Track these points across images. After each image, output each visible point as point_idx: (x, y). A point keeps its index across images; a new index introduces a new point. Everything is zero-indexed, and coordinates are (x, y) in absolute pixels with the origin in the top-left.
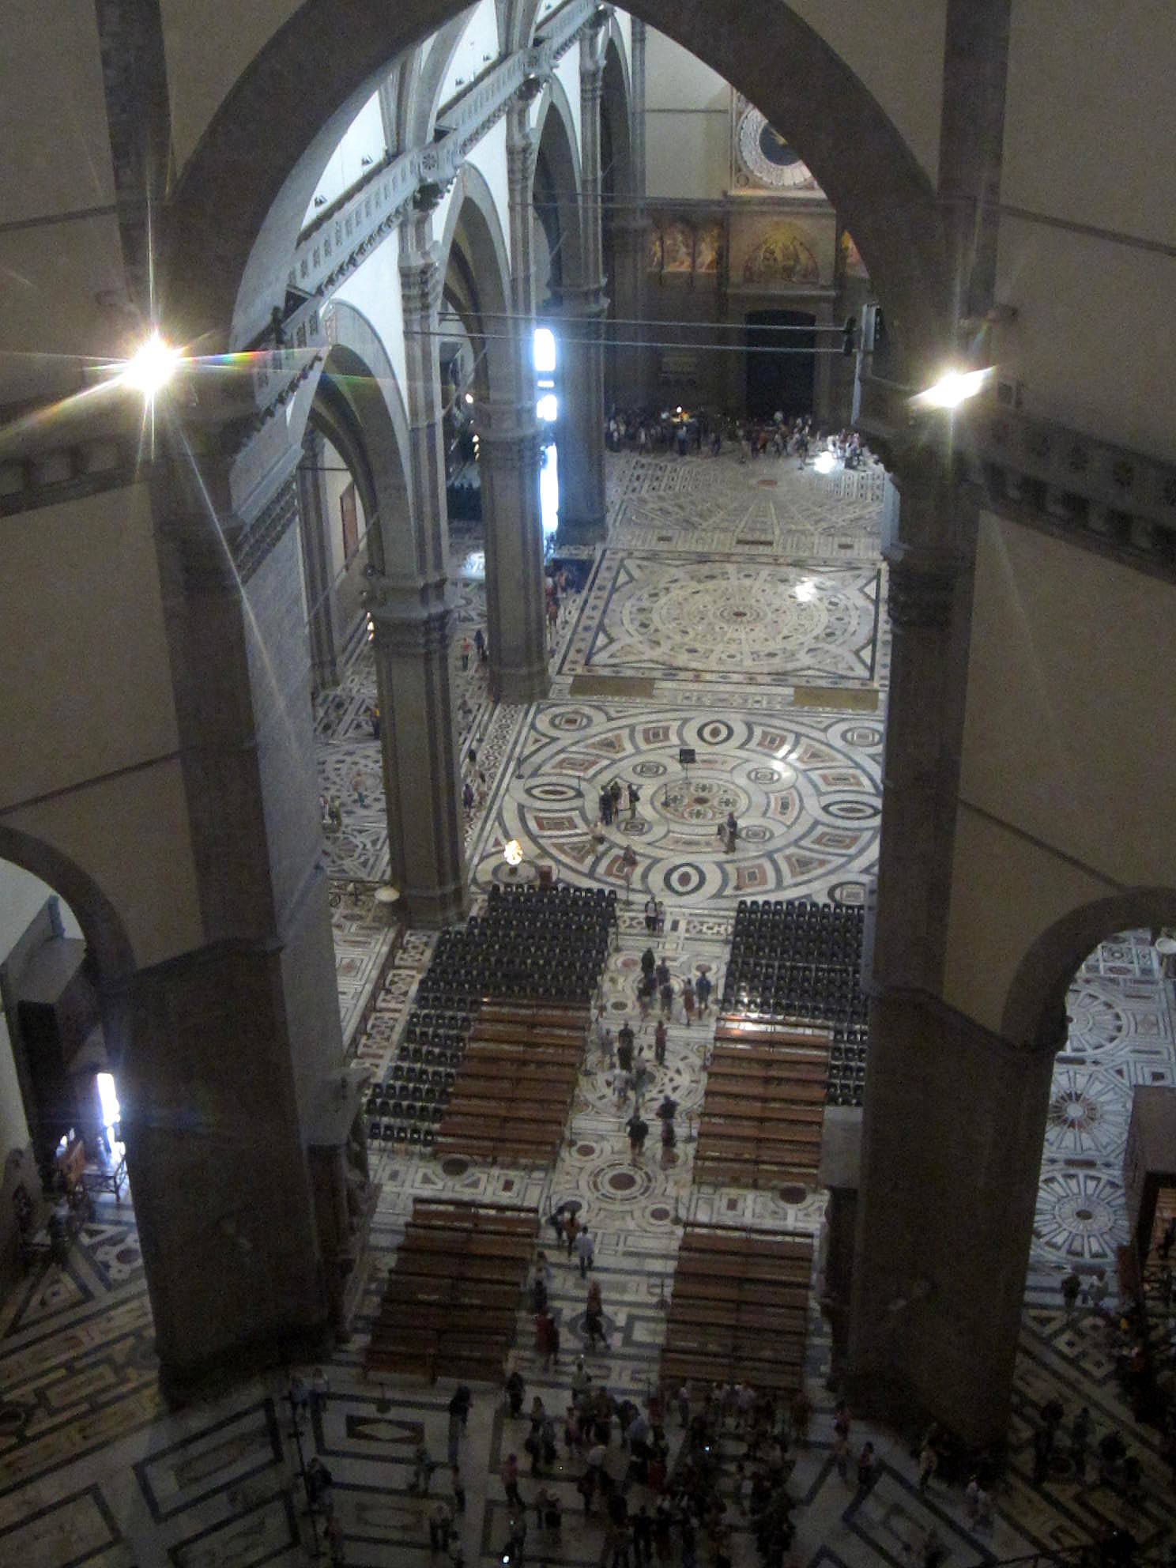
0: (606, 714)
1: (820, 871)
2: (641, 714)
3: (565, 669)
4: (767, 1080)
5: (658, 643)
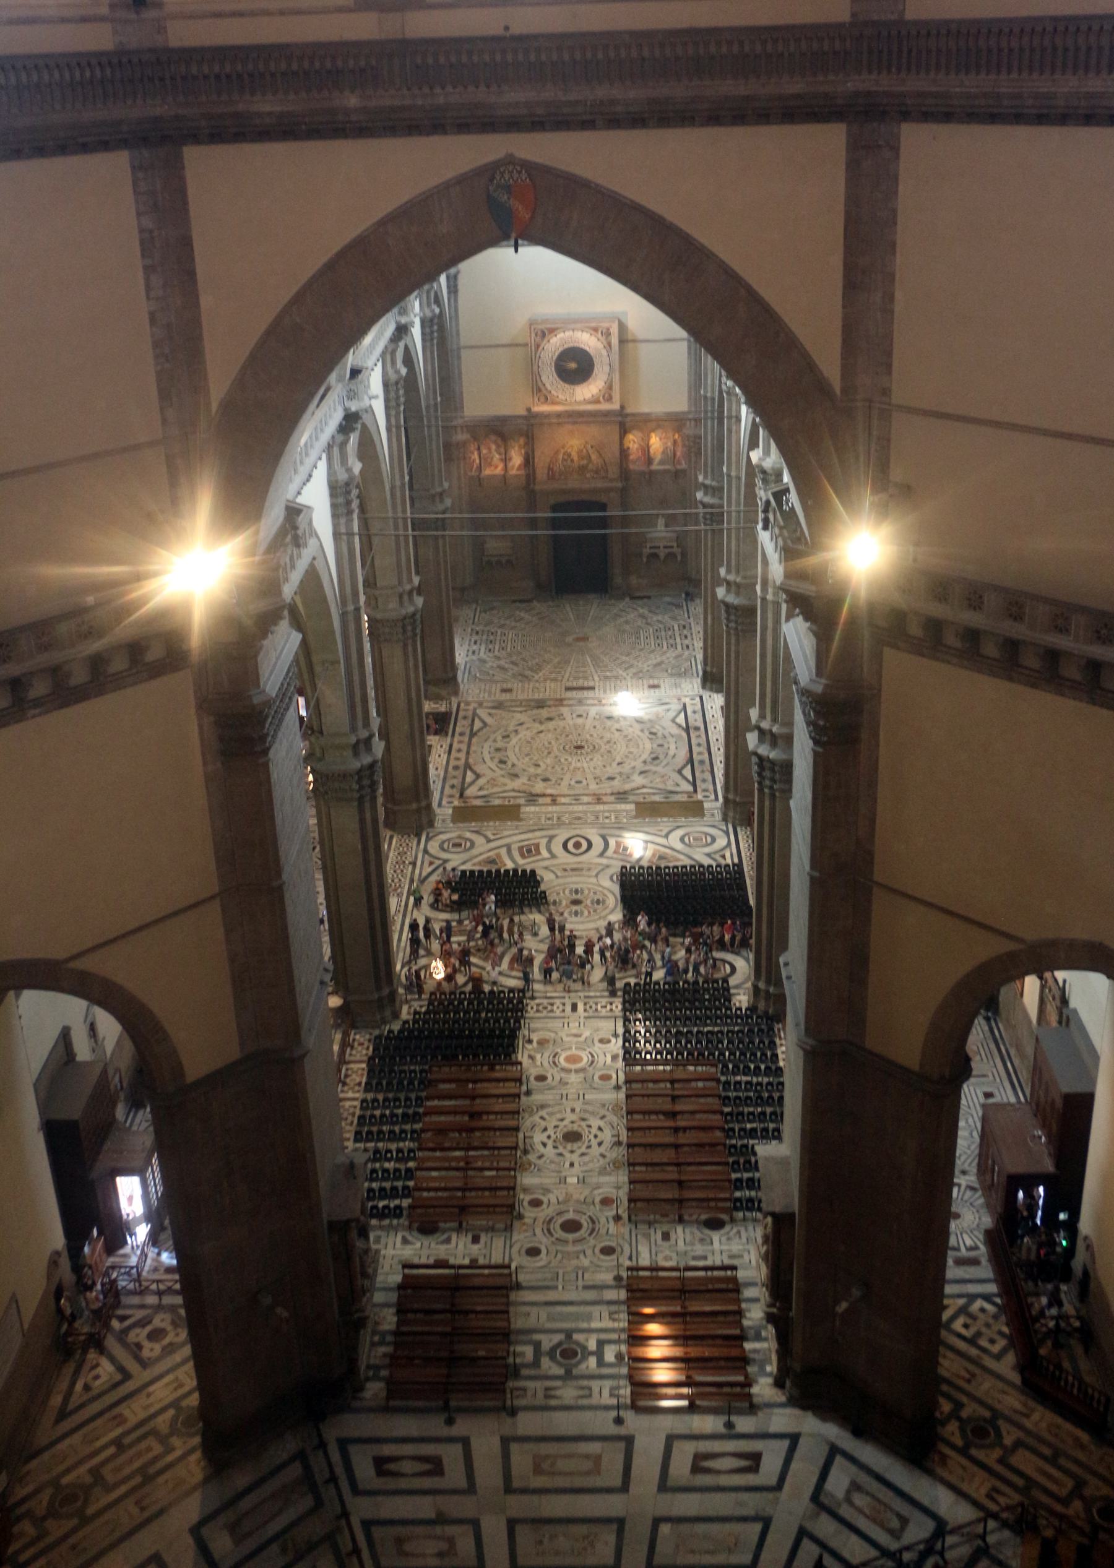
0: (485, 837)
3: (444, 803)
4: (676, 1130)
5: (516, 776)
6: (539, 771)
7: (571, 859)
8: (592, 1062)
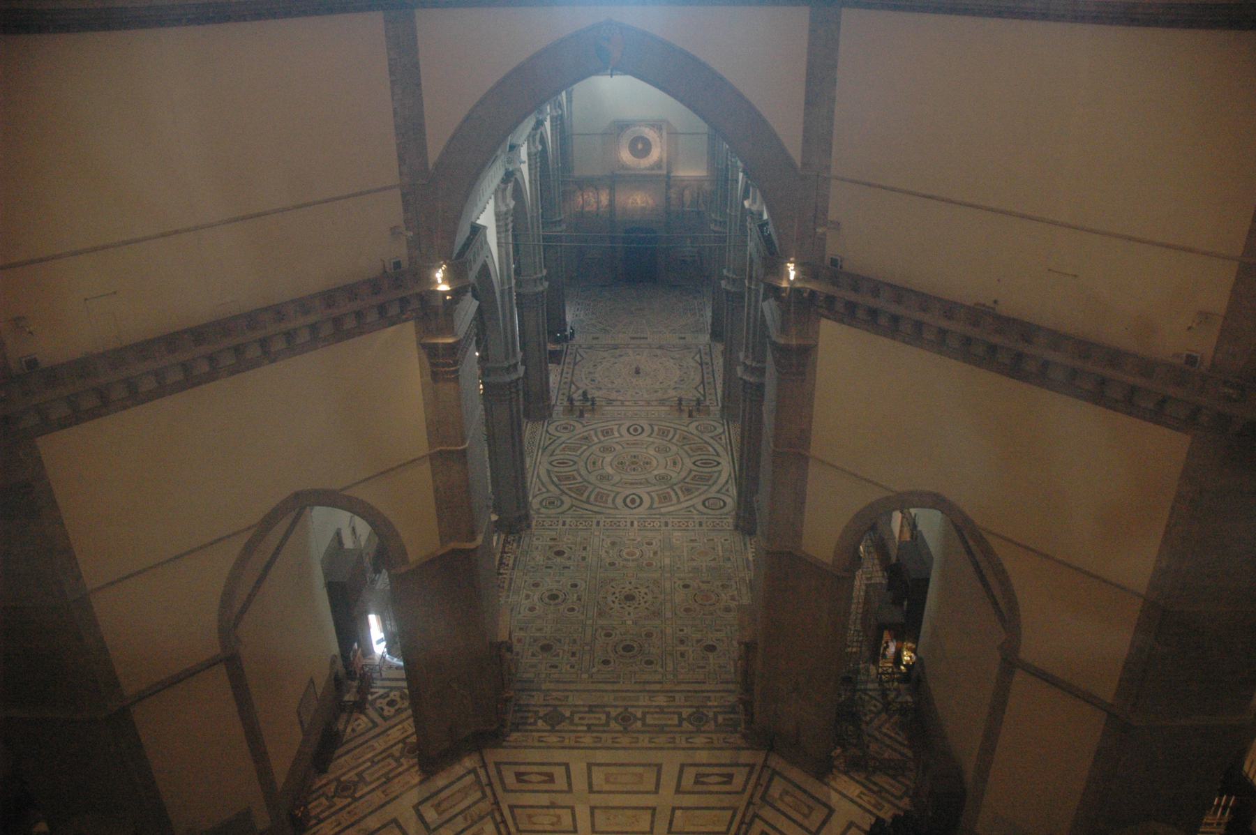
1: (697, 493)
5: (601, 389)
6: (614, 386)
7: (631, 438)
8: (642, 555)
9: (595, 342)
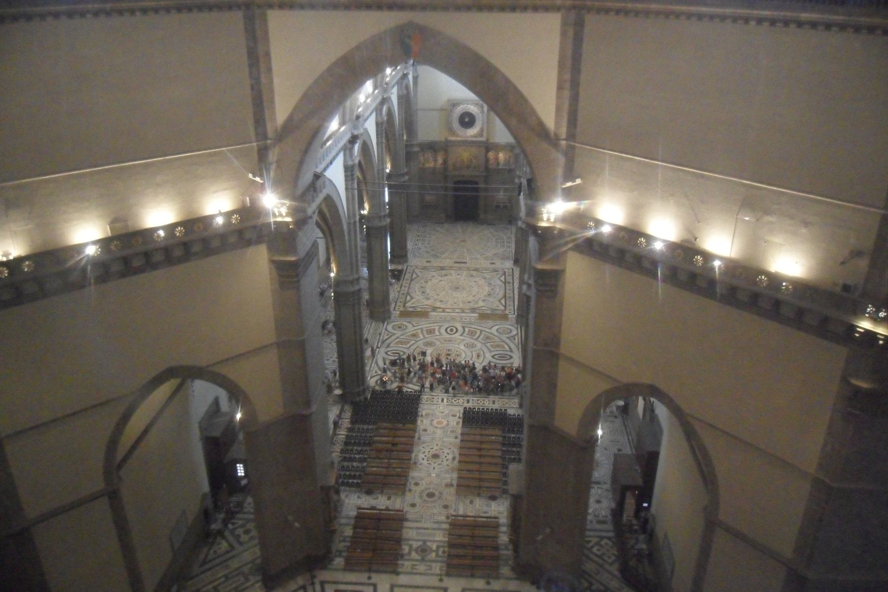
0: (412, 324)
2: (424, 324)
3: (396, 309)
4: (480, 456)
5: (429, 299)
6: (439, 297)
7: (448, 336)
8: (448, 424)
9: (428, 264)
